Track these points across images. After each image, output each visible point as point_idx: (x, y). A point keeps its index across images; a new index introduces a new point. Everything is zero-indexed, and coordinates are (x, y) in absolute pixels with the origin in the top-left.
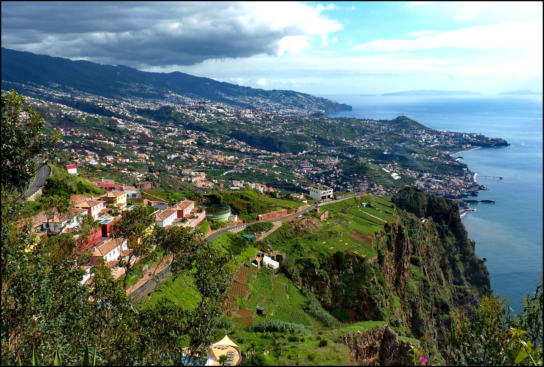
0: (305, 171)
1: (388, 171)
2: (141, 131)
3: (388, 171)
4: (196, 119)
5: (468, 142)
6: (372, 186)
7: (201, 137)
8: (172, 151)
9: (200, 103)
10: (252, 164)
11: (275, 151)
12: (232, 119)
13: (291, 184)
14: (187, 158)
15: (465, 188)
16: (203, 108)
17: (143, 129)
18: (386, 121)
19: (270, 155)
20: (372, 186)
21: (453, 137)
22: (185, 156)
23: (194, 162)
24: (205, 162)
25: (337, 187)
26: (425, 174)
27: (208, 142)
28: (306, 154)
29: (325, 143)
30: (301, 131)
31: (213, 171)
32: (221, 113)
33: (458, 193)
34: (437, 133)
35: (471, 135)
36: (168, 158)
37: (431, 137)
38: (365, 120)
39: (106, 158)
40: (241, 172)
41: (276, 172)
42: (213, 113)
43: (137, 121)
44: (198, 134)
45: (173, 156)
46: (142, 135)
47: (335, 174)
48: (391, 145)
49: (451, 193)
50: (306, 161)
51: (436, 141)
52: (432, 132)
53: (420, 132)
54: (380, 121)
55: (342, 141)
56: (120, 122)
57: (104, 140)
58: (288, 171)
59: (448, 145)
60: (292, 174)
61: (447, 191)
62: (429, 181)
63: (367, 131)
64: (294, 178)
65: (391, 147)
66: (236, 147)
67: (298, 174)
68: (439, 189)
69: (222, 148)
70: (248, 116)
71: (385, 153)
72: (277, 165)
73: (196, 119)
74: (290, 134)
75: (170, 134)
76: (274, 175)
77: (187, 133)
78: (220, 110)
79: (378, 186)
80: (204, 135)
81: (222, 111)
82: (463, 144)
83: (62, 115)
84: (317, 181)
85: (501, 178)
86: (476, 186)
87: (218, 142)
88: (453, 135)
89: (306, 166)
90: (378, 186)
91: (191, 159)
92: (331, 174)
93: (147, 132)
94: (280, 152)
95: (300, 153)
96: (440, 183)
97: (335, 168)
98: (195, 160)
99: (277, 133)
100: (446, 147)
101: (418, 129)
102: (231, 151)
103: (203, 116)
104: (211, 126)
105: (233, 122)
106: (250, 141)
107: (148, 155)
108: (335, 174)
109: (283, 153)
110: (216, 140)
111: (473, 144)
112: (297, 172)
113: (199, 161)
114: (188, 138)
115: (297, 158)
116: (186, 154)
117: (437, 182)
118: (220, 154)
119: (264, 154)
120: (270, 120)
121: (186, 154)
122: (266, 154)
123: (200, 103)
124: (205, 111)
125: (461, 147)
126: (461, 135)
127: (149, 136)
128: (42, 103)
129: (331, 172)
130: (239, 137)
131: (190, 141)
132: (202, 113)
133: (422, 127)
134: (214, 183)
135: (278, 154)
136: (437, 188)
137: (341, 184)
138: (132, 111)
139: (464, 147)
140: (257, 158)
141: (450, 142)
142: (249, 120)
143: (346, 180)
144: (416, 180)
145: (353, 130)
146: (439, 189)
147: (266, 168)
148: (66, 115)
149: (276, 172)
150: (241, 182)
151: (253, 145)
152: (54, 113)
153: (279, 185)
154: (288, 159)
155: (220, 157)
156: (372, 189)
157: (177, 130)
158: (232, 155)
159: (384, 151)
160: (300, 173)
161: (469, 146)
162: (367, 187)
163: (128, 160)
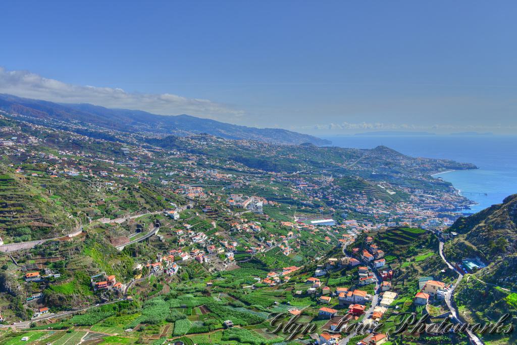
0: (302, 188)
1: (383, 187)
2: (143, 154)
3: (383, 187)
4: (198, 147)
5: (443, 166)
6: (371, 200)
7: (201, 159)
8: (171, 169)
9: (201, 134)
10: (250, 181)
11: (272, 171)
12: (230, 146)
13: (290, 199)
14: (185, 175)
15: (458, 202)
16: (204, 138)
17: (146, 152)
18: (367, 150)
19: (267, 174)
20: (371, 200)
21: (428, 162)
22: (184, 173)
23: (193, 178)
24: (203, 179)
25: (336, 201)
26: (417, 191)
27: (207, 163)
28: (300, 174)
29: (317, 165)
30: (293, 156)
31: (211, 185)
32: (221, 142)
33: (453, 207)
34: (414, 159)
35: (444, 161)
36: (167, 175)
37: (409, 162)
38: (348, 149)
39: (100, 173)
40: (239, 187)
41: (274, 188)
42: (213, 142)
43: (143, 147)
44: (198, 156)
45: (171, 174)
46: (145, 157)
47: (332, 190)
48: (377, 167)
49: (446, 206)
50: (301, 179)
51: (414, 165)
52: (409, 158)
53: (398, 158)
54: (364, 150)
55: (332, 164)
56: (125, 146)
57: (106, 159)
58: (285, 187)
59: (426, 168)
60: (289, 190)
61: (442, 205)
62: (422, 196)
63: (353, 156)
64: (292, 193)
65: (377, 168)
66: (234, 167)
67: (295, 190)
68: (434, 203)
69: (221, 168)
70: (245, 144)
71: (373, 173)
72: (274, 181)
73: (198, 147)
74: (284, 158)
75: (172, 157)
76: (272, 190)
77: (188, 156)
78: (220, 140)
79: (377, 200)
80: (204, 157)
81: (222, 140)
82: (439, 167)
83: (70, 140)
84: (315, 195)
85: (486, 194)
86: (467, 201)
87: (217, 163)
88: (428, 160)
89: (302, 183)
90: (377, 200)
91: (189, 175)
92: (328, 189)
93: (150, 154)
94: (275, 172)
95: (294, 173)
96: (433, 198)
97: (332, 184)
98: (194, 176)
99: (272, 157)
100: (424, 170)
101: (397, 156)
102: (230, 170)
103: (203, 144)
104: (211, 151)
105: (230, 149)
106: (247, 162)
107: (147, 172)
108: (332, 190)
109: (279, 172)
110: (216, 161)
111: (448, 168)
112: (294, 188)
113: (198, 178)
114: (189, 160)
115: (293, 176)
116: (185, 172)
117: (429, 197)
118: (219, 173)
119: (260, 173)
120: (265, 147)
121: (185, 172)
122: (260, 173)
123: (201, 134)
124: (206, 140)
125: (437, 170)
126: (435, 161)
127: (151, 157)
128: (54, 130)
129: (328, 188)
130: (238, 160)
131: (190, 162)
132: (204, 141)
133: (400, 155)
134: (211, 196)
135: (273, 173)
136: (432, 202)
137: (339, 198)
138: (140, 140)
139: (440, 169)
140: (254, 177)
141: (427, 166)
142: (246, 147)
143: (344, 195)
144: (410, 195)
145: (340, 155)
146: (434, 203)
147: (264, 184)
148: (74, 140)
149: (274, 188)
150: (239, 196)
151: (250, 166)
152: (63, 139)
153: (276, 199)
154: (284, 177)
155: (217, 175)
156: (372, 203)
157: (179, 153)
158: (230, 174)
159: (372, 172)
160: (297, 188)
161: (444, 169)
162: (366, 201)
163: (122, 176)
